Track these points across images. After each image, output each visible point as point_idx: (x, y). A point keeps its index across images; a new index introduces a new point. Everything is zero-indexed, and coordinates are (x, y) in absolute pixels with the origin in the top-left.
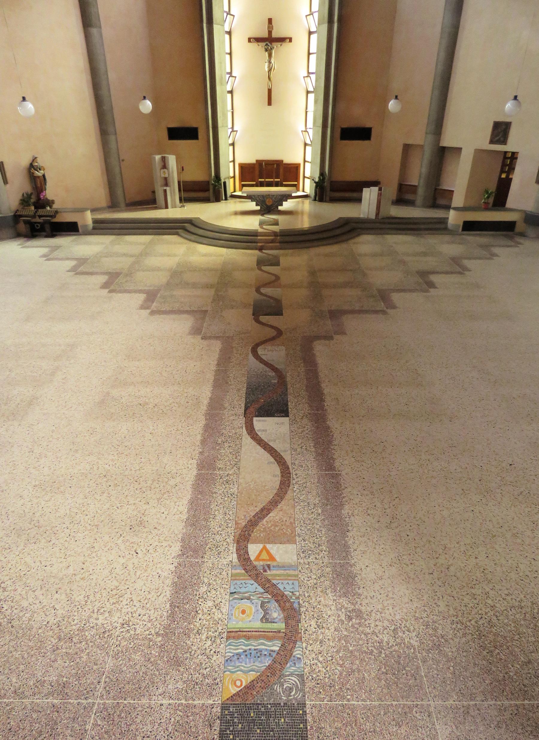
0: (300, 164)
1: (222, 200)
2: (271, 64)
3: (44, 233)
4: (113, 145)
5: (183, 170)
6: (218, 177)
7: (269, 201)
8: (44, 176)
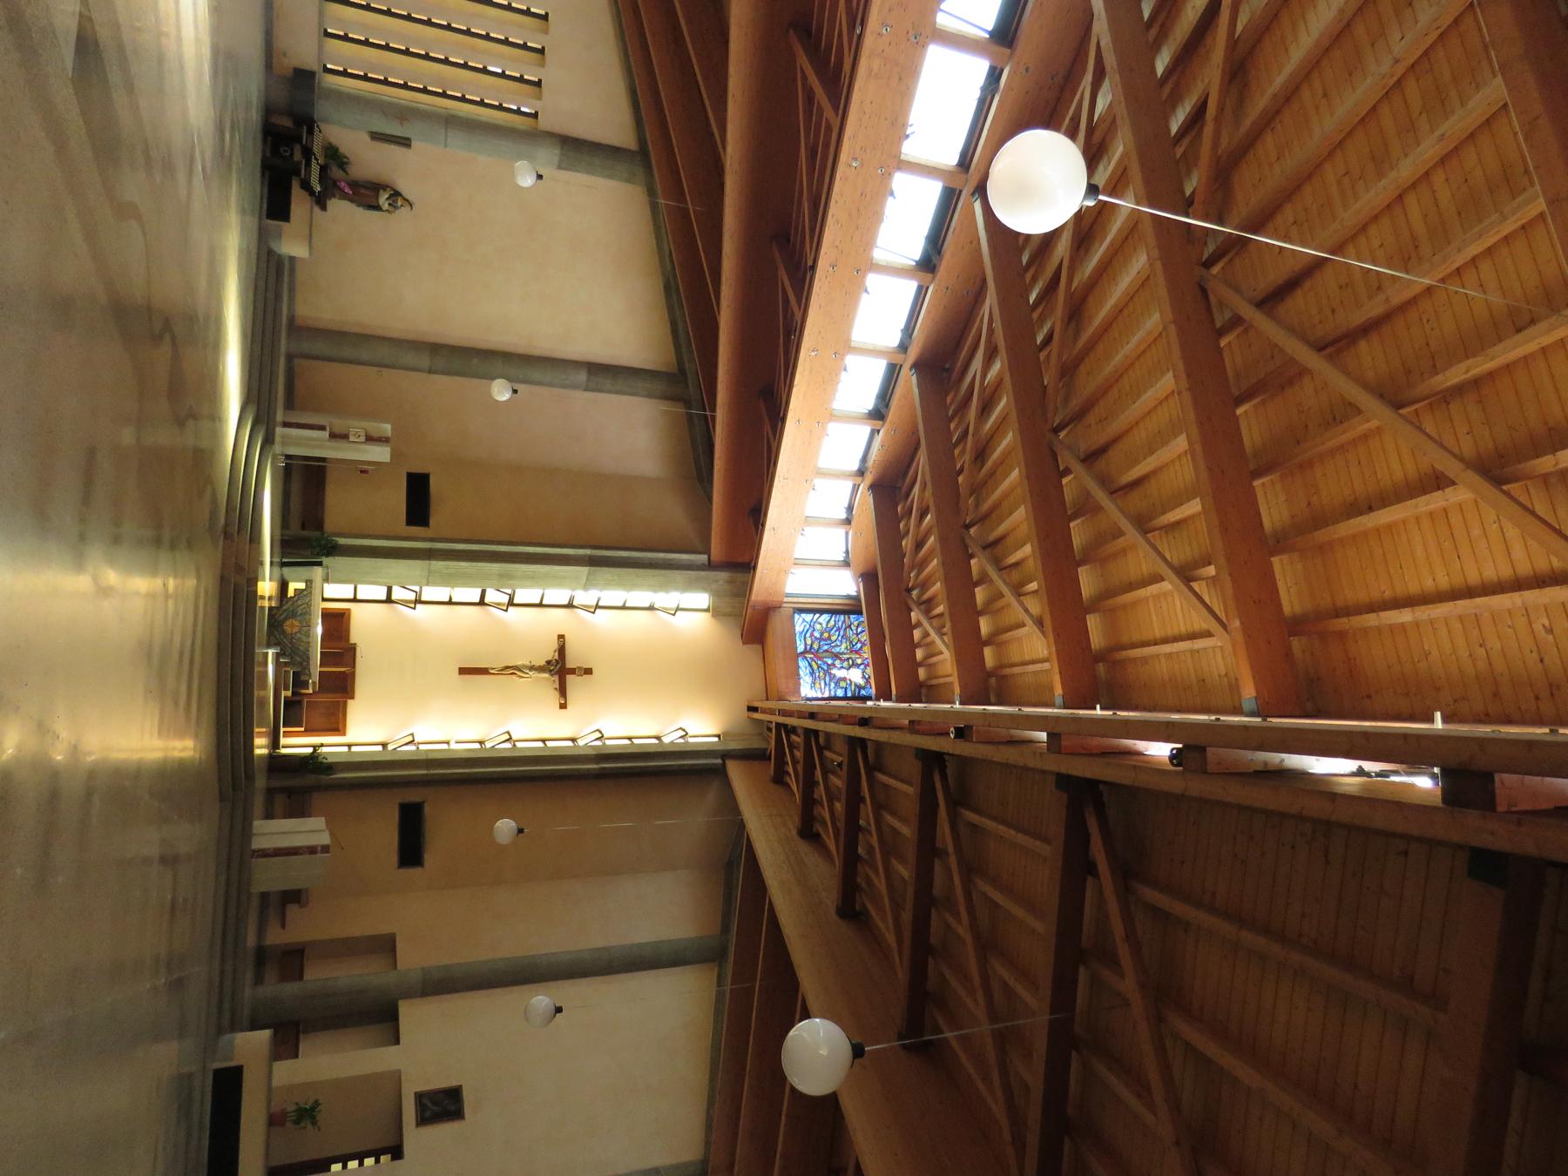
0: (344, 734)
1: (283, 557)
2: (527, 671)
3: (268, 154)
4: (410, 358)
5: (362, 472)
6: (333, 550)
7: (293, 626)
8: (377, 208)
